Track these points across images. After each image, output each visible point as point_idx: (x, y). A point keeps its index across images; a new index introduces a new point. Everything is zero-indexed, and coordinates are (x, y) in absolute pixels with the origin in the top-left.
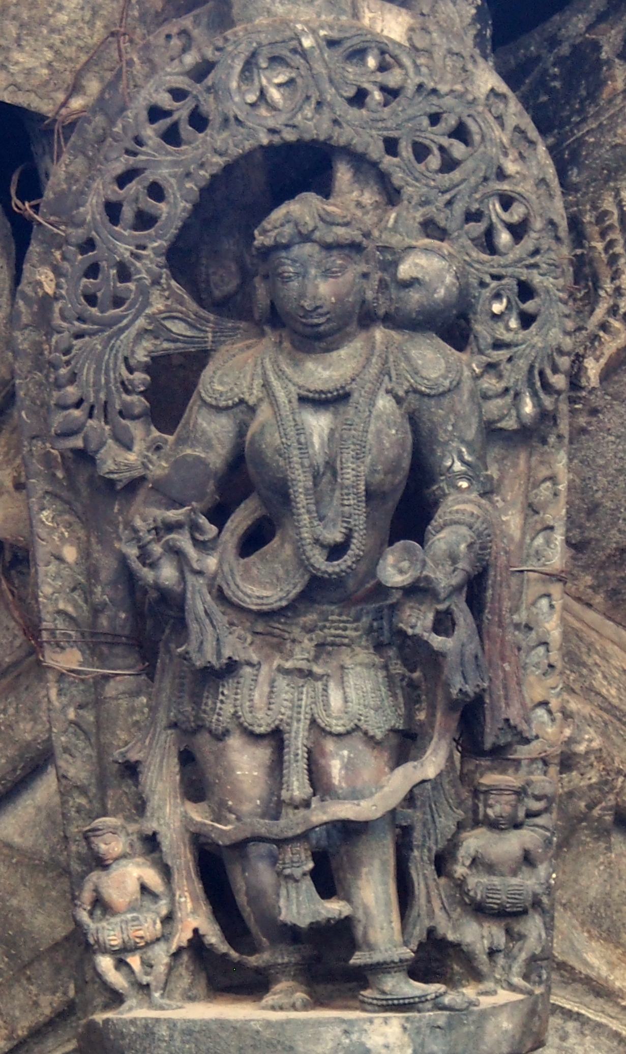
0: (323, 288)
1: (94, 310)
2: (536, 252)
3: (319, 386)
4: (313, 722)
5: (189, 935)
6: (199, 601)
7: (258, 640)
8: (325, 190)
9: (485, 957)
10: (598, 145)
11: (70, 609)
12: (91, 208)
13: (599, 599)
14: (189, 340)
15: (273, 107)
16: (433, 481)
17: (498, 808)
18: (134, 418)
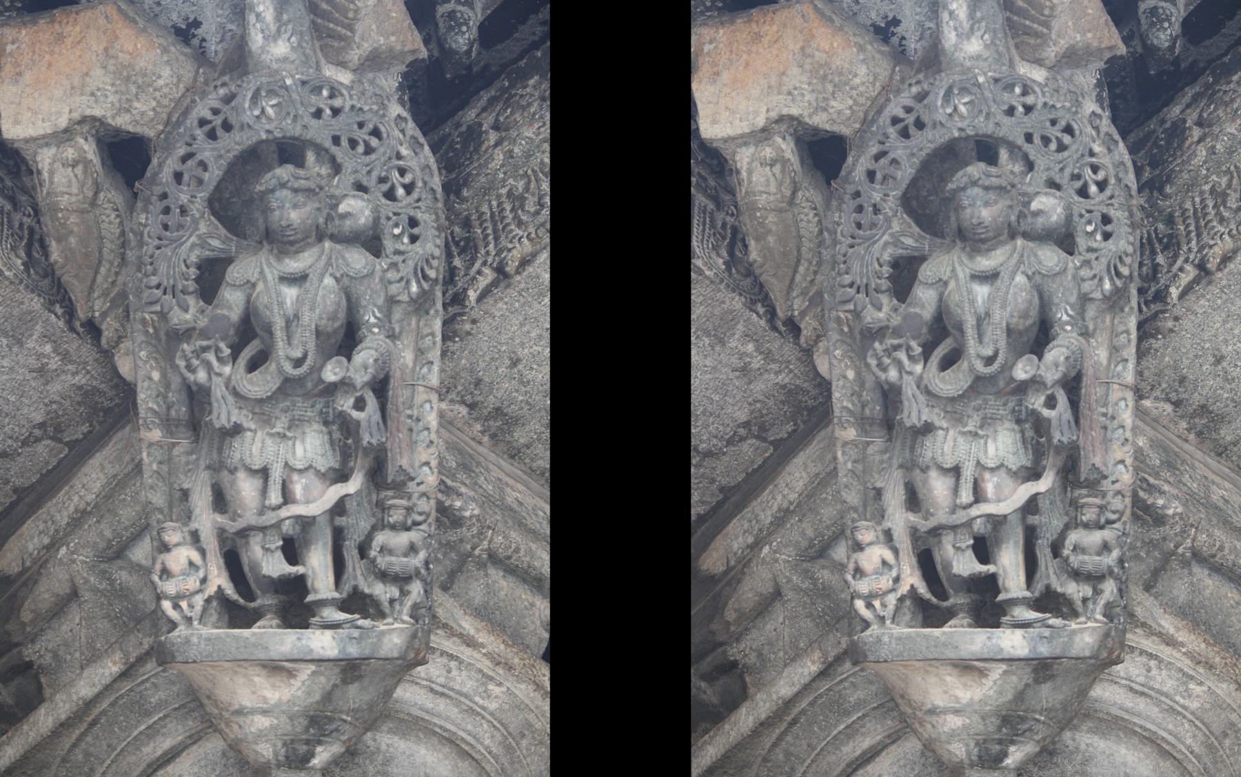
0: (294, 214)
1: (168, 234)
2: (419, 200)
3: (291, 270)
4: (286, 464)
5: (215, 589)
6: (219, 390)
7: (256, 417)
8: (300, 164)
9: (386, 604)
10: (478, 174)
11: (155, 407)
12: (166, 175)
13: (486, 439)
14: (222, 250)
15: (269, 119)
16: (359, 329)
17: (396, 517)
18: (189, 294)
